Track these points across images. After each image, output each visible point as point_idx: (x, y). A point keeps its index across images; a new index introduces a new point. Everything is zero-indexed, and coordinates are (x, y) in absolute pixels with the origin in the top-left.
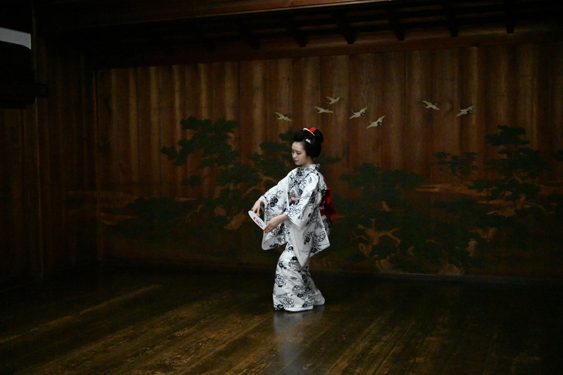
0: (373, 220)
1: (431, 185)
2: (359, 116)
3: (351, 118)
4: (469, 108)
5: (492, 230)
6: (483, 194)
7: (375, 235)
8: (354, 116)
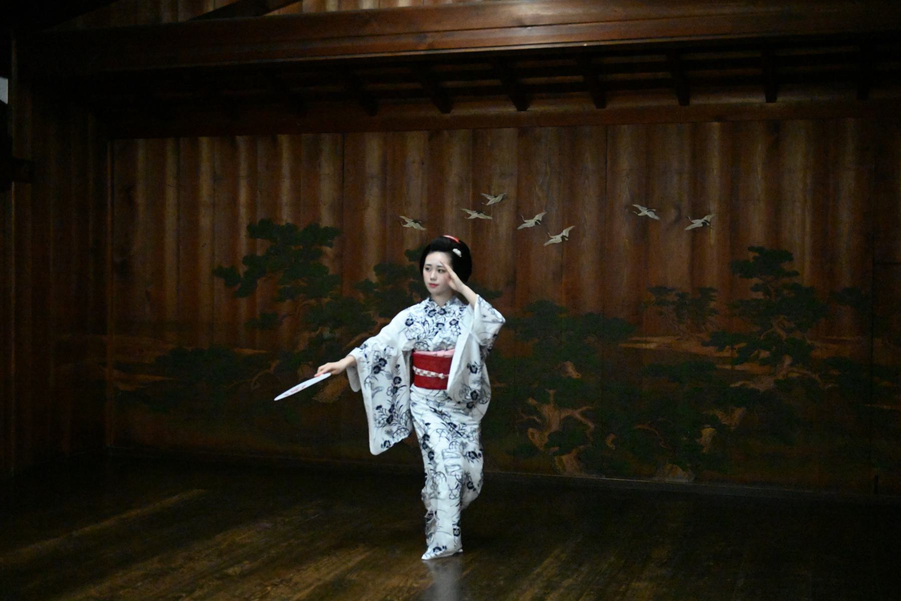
0: (551, 392)
2: (532, 226)
3: (521, 227)
4: (706, 218)
5: (739, 412)
6: (726, 354)
7: (553, 416)
8: (524, 225)
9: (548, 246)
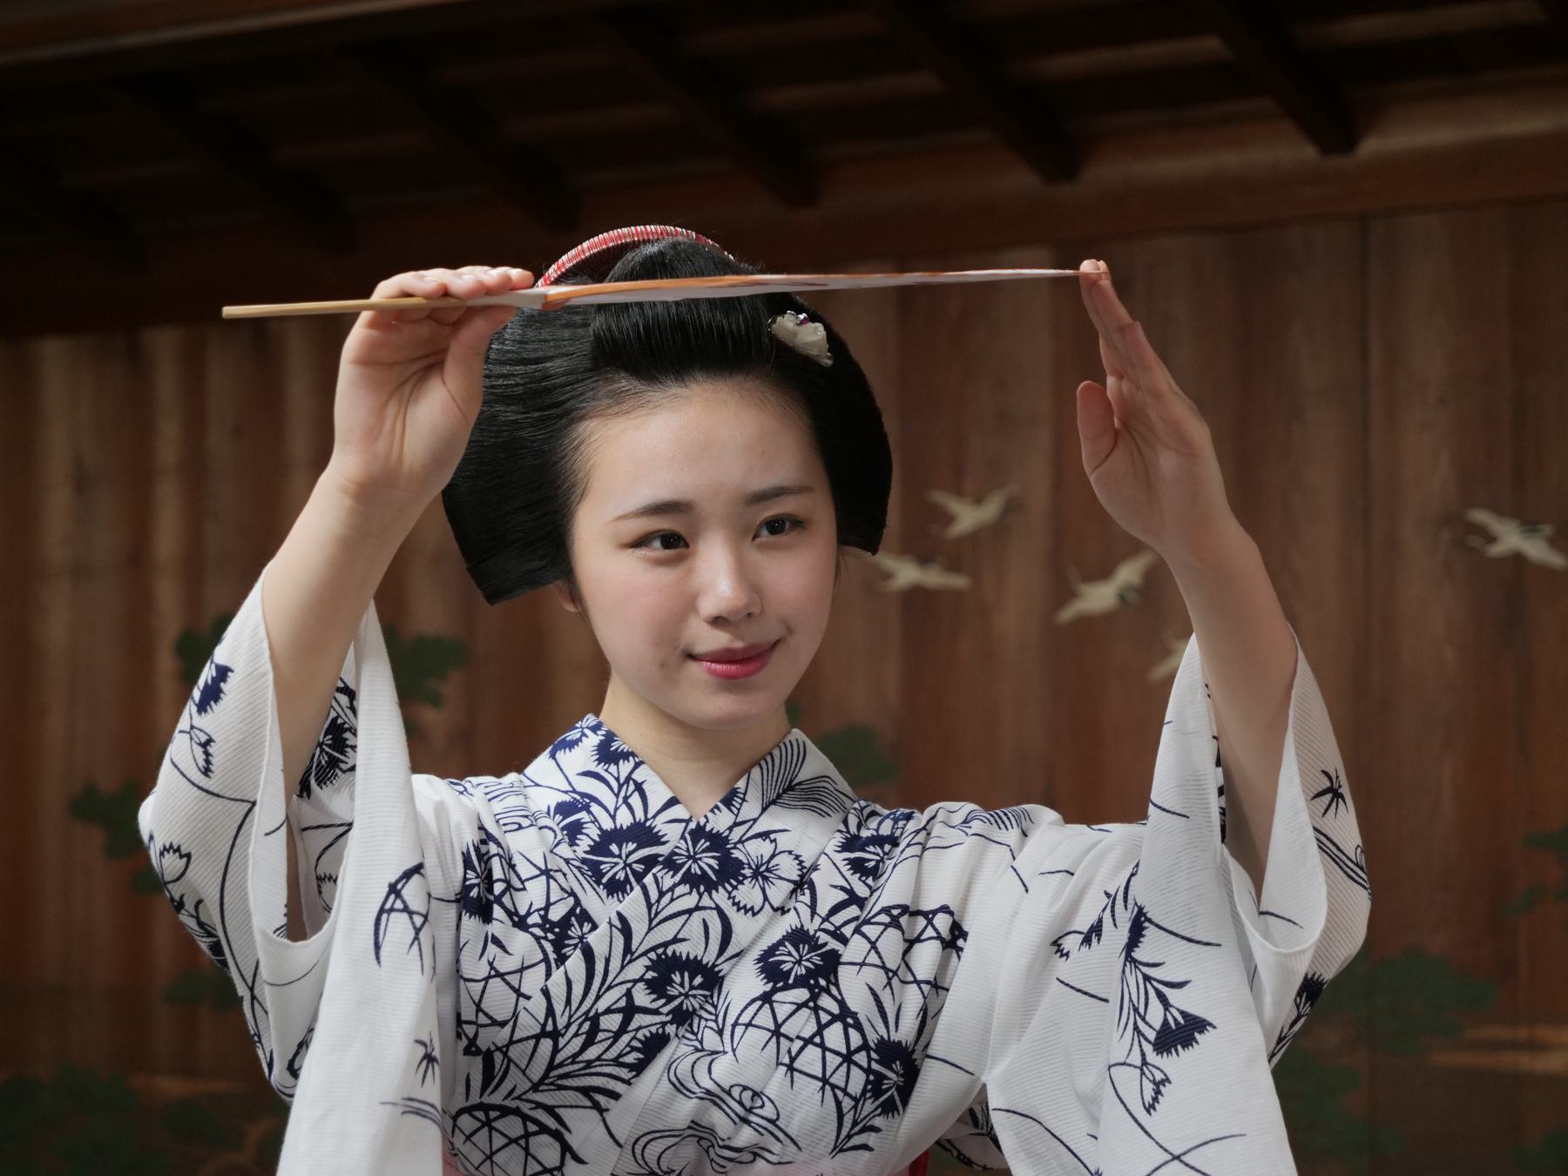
1: (1522, 1033)
3: (1067, 614)
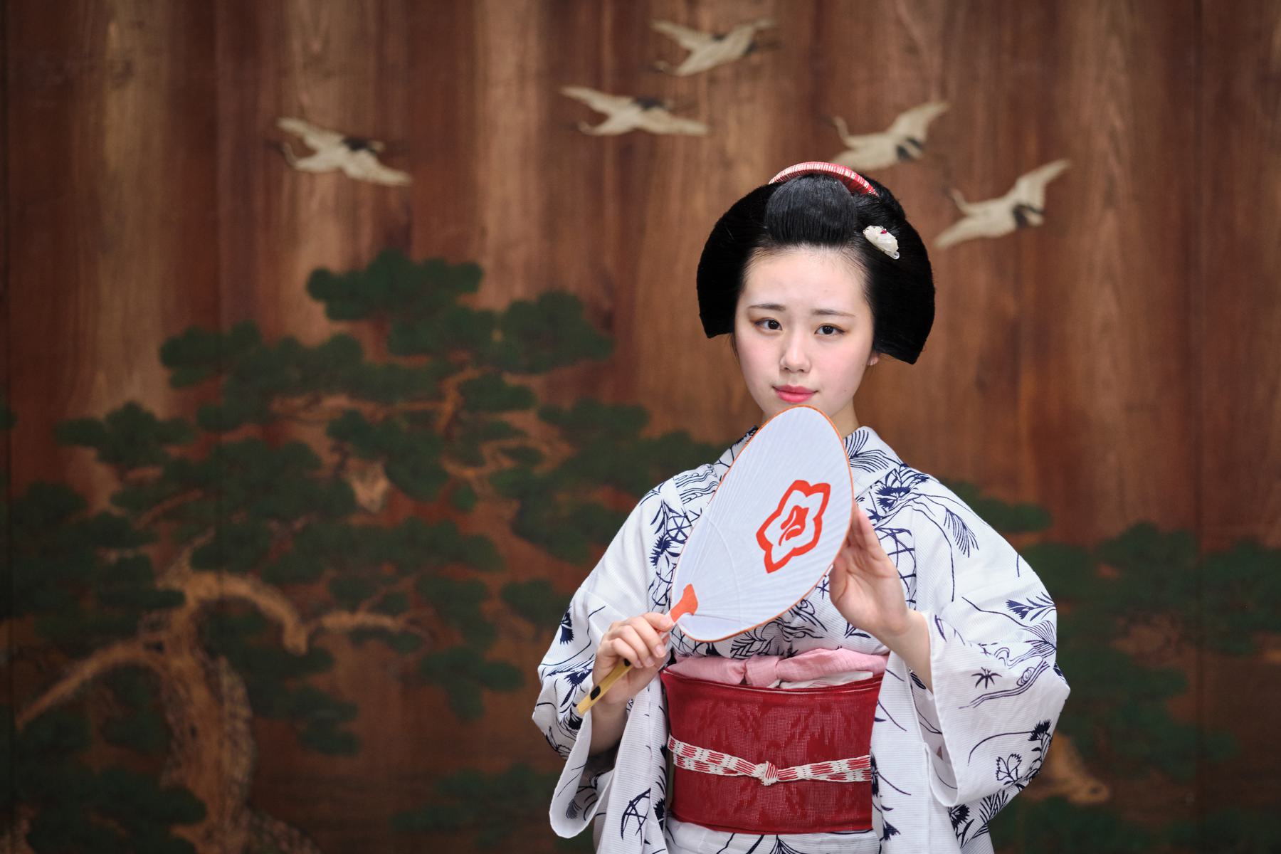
9: (955, 248)
